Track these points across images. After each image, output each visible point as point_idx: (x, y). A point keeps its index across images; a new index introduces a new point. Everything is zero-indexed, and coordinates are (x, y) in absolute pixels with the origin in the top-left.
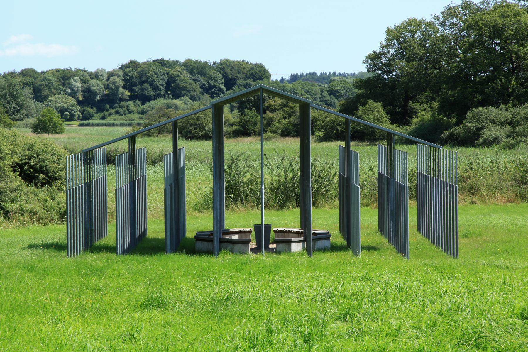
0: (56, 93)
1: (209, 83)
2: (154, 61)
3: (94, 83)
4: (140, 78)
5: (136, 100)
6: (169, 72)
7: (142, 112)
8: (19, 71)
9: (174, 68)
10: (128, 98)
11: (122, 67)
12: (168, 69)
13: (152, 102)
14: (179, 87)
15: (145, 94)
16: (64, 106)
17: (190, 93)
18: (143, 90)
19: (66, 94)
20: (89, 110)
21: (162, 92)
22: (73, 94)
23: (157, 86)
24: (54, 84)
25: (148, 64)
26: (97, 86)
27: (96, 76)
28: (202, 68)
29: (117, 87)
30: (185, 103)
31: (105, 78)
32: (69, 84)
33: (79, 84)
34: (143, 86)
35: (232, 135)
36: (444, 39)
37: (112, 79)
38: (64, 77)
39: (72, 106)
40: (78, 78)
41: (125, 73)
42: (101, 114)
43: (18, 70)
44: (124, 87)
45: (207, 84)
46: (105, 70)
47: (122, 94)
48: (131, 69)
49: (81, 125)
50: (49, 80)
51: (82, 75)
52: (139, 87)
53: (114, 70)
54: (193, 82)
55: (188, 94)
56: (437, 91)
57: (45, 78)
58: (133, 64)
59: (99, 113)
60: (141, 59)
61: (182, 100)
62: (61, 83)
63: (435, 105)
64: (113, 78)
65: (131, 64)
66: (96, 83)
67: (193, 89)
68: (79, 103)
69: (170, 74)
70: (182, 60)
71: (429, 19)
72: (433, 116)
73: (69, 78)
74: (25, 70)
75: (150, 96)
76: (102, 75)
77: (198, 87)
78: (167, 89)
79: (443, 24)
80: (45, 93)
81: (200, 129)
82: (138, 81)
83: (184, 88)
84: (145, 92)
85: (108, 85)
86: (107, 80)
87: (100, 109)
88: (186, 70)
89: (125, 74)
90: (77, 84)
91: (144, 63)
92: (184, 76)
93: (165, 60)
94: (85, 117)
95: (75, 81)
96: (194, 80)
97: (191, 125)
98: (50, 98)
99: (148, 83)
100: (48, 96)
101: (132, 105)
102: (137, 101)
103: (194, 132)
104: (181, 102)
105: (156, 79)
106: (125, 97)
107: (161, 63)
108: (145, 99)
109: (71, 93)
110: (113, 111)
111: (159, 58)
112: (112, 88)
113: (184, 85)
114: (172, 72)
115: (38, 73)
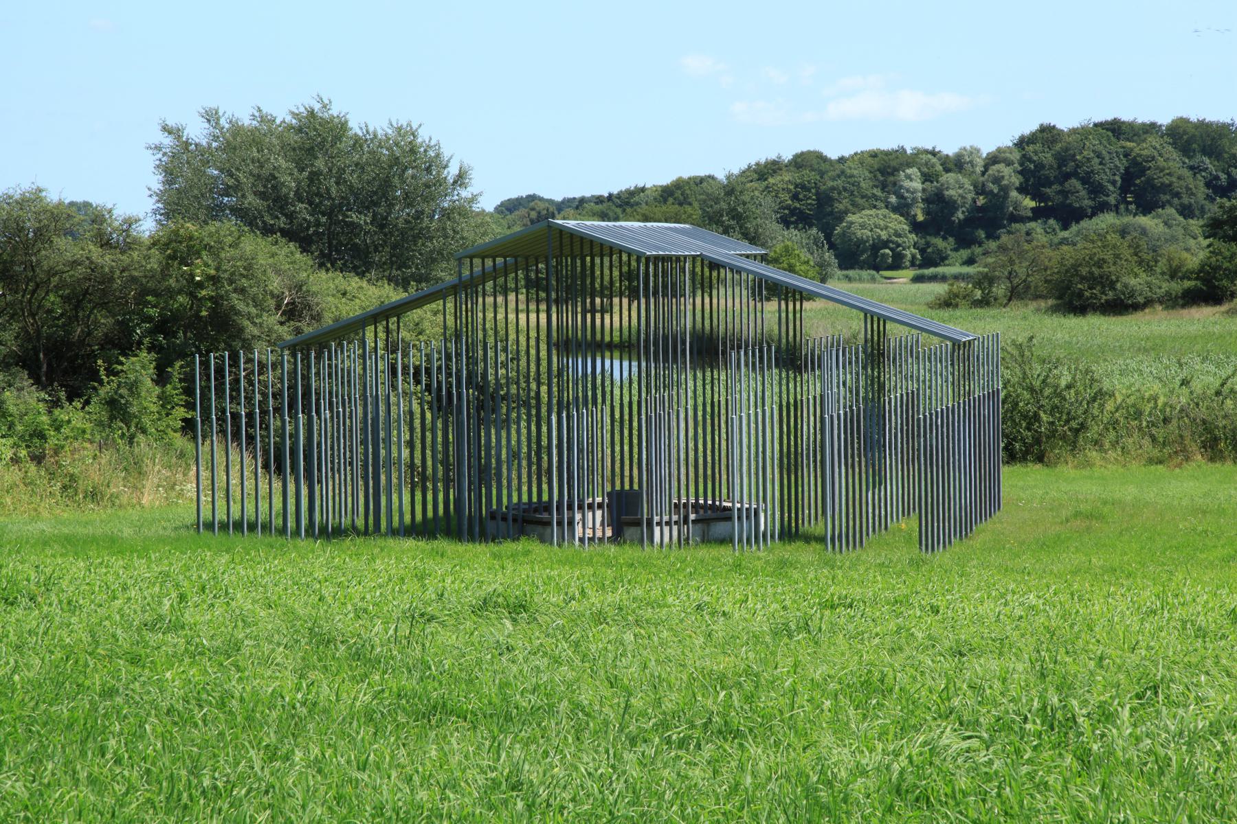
0: (866, 205)
1: (1229, 174)
2: (1096, 125)
3: (952, 181)
4: (1059, 167)
5: (1048, 218)
6: (1132, 150)
8: (791, 157)
9: (1144, 140)
10: (1030, 214)
11: (1022, 143)
12: (1129, 144)
13: (1085, 223)
14: (1153, 187)
15: (1070, 205)
16: (879, 236)
17: (1180, 198)
19: (887, 207)
20: (939, 242)
21: (1112, 200)
22: (902, 208)
23: (1100, 185)
24: (863, 185)
25: (1082, 133)
26: (958, 187)
27: (957, 164)
28: (1213, 139)
29: (1005, 190)
30: (1166, 223)
31: (979, 169)
32: (895, 184)
33: (917, 185)
34: (1067, 185)
35: (1181, 302)
37: (993, 170)
38: (886, 167)
39: (899, 236)
40: (915, 170)
41: (1024, 156)
42: (964, 253)
43: (787, 156)
44: (1022, 190)
45: (1223, 177)
46: (978, 151)
47: (1017, 205)
48: (1038, 147)
49: (918, 279)
50: (852, 176)
51: (926, 164)
52: (1056, 187)
53: (999, 150)
54: (1187, 173)
55: (1176, 201)
57: (843, 172)
58: (1047, 134)
59: (962, 251)
60: (1066, 121)
61: (1159, 216)
62: (877, 183)
64: (996, 167)
65: (1039, 135)
66: (957, 181)
67: (1188, 189)
68: (916, 227)
69: (1133, 154)
70: (1164, 119)
73: (896, 170)
74: (802, 153)
75: (1081, 207)
76: (971, 162)
77: (1202, 184)
78: (1124, 190)
80: (841, 207)
81: (1103, 287)
83: (1166, 188)
84: (1071, 199)
85: (983, 185)
86: (983, 174)
87: (964, 241)
88: (1174, 144)
89: (1025, 158)
90: (913, 183)
91: (1074, 131)
92: (1166, 160)
93: (1124, 123)
94: (930, 259)
95: (909, 177)
96: (1191, 168)
97: (1083, 278)
98: (851, 218)
99: (1079, 179)
100: (846, 212)
101: (1039, 230)
102: (1052, 222)
103: (1087, 294)
104: (1156, 221)
105: (1097, 167)
106: (1023, 213)
107: (1113, 131)
108: (1068, 216)
109: (899, 204)
110: (993, 245)
111: (1110, 118)
112: (992, 191)
113: (1166, 180)
114: (1137, 150)
115: (830, 160)
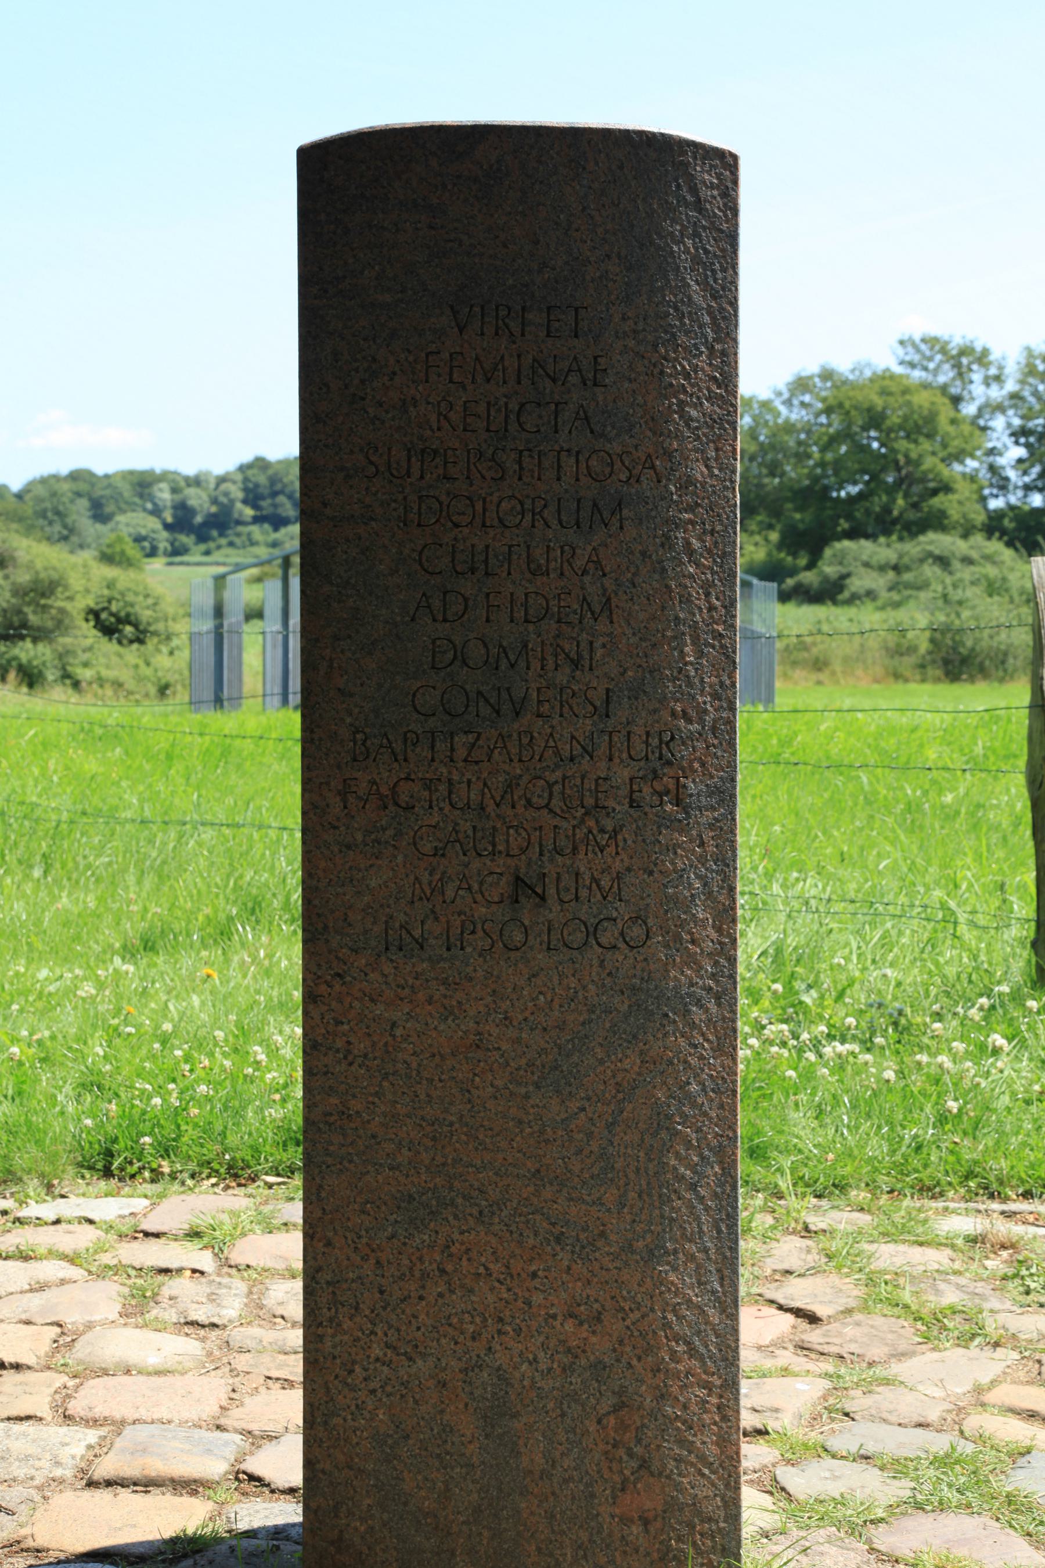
7: (274, 545)
11: (242, 468)
18: (275, 506)
22: (156, 512)
26: (199, 500)
27: (196, 481)
29: (232, 502)
31: (212, 486)
32: (150, 494)
36: (789, 428)
37: (224, 487)
38: (143, 484)
42: (203, 547)
44: (245, 502)
47: (241, 513)
48: (255, 471)
53: (228, 473)
56: (776, 513)
63: (774, 536)
68: (167, 527)
71: (764, 395)
72: (769, 554)
79: (788, 403)
82: (266, 492)
84: (280, 511)
87: (202, 537)
89: (246, 480)
90: (164, 495)
91: (280, 462)
110: (223, 541)
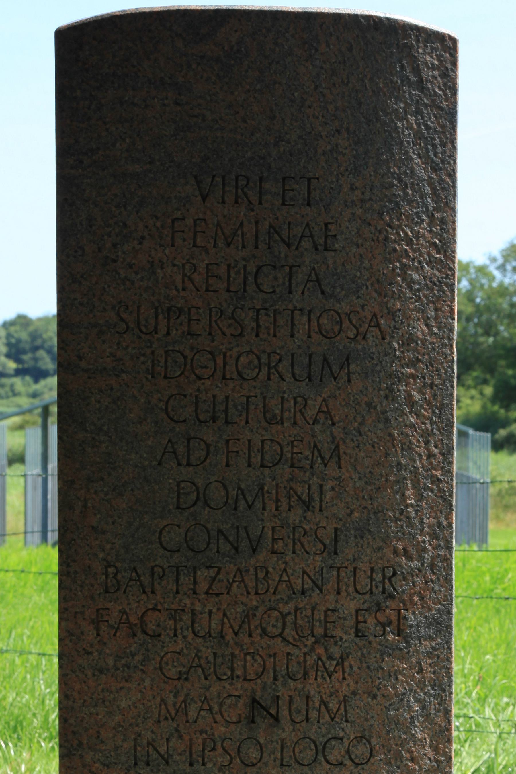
7: (34, 395)
18: (36, 360)
36: (503, 291)
48: (18, 328)
56: (491, 369)
63: (489, 390)
71: (480, 260)
72: (484, 407)
79: (502, 268)
82: (27, 347)
89: (9, 336)
91: (40, 320)
